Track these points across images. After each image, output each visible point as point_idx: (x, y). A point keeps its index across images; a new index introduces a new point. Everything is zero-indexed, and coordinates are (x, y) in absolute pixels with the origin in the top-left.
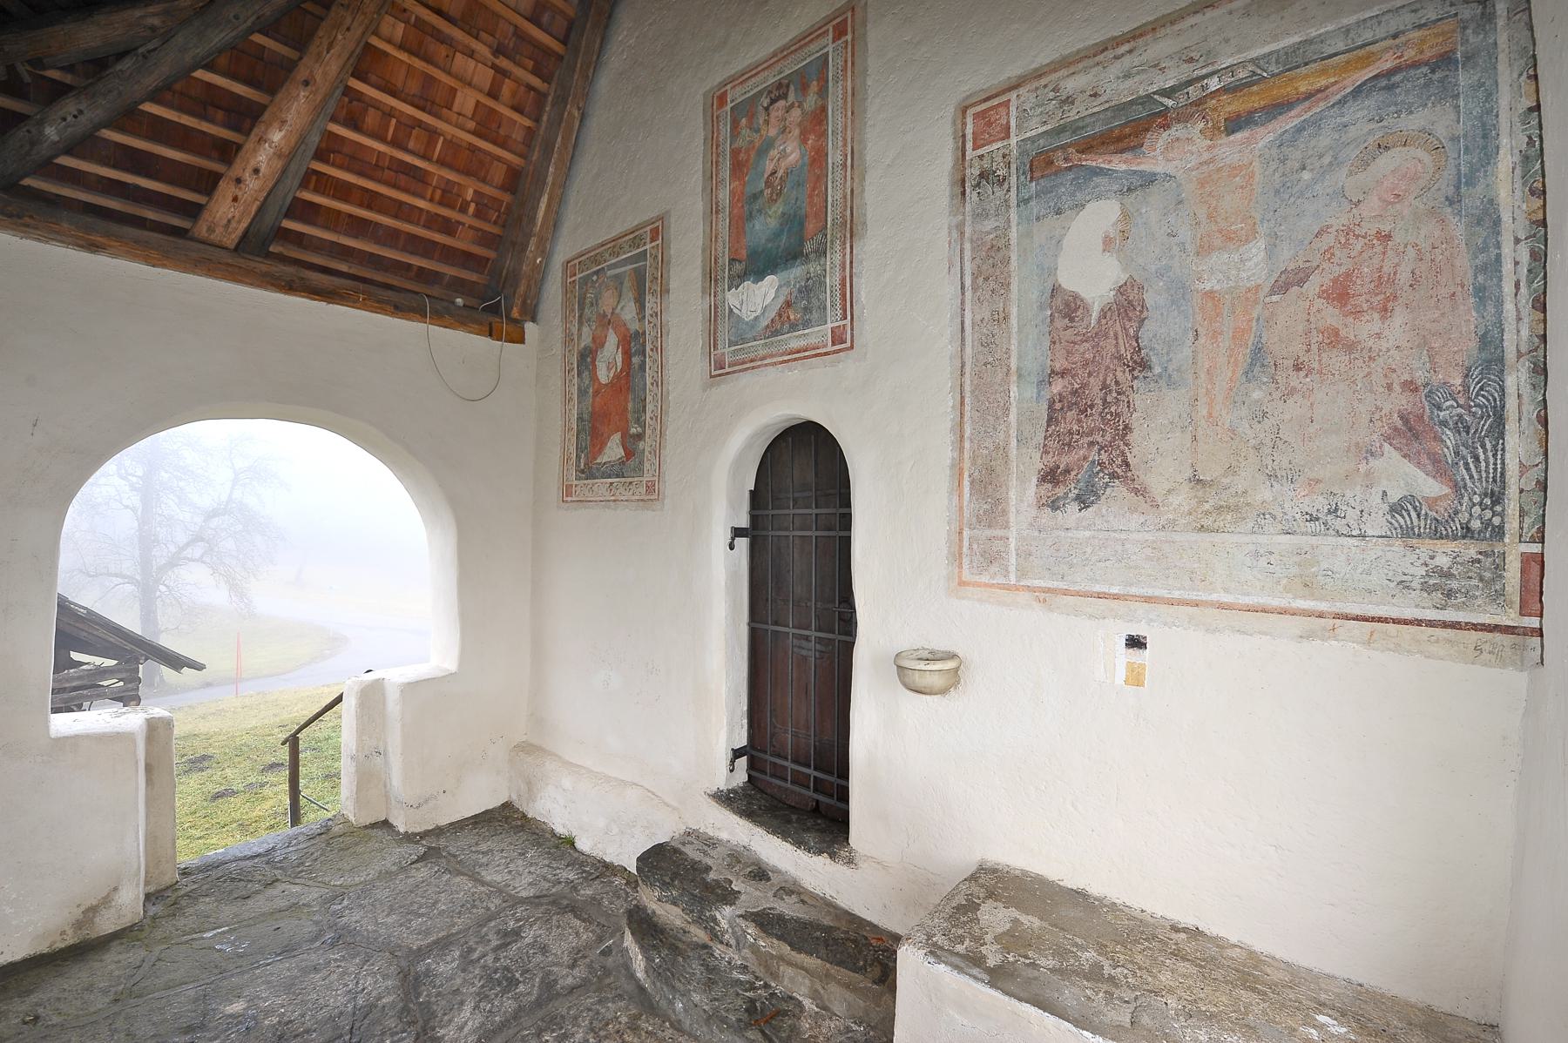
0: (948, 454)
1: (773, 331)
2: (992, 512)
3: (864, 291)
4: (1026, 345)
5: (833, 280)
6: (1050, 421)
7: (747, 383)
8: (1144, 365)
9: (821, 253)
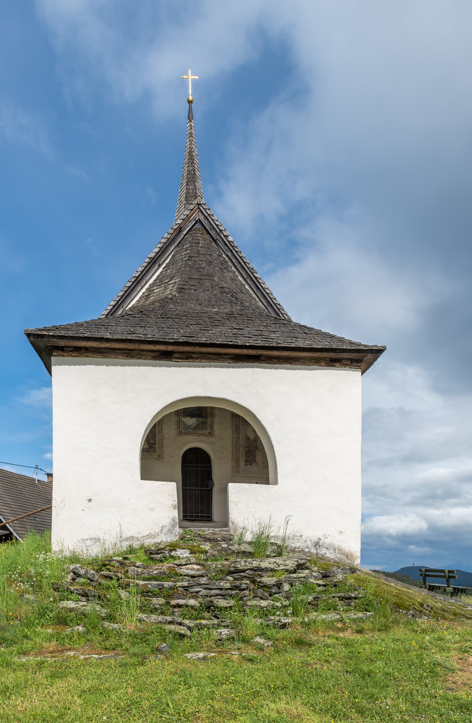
0: (231, 457)
1: (195, 428)
2: (238, 465)
3: (216, 427)
4: (242, 442)
5: (209, 423)
6: (246, 453)
7: (189, 438)
8: (257, 448)
9: (206, 417)
